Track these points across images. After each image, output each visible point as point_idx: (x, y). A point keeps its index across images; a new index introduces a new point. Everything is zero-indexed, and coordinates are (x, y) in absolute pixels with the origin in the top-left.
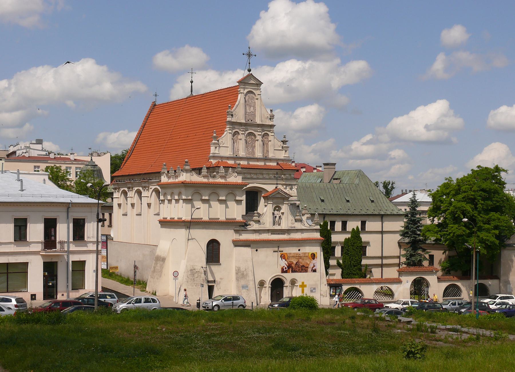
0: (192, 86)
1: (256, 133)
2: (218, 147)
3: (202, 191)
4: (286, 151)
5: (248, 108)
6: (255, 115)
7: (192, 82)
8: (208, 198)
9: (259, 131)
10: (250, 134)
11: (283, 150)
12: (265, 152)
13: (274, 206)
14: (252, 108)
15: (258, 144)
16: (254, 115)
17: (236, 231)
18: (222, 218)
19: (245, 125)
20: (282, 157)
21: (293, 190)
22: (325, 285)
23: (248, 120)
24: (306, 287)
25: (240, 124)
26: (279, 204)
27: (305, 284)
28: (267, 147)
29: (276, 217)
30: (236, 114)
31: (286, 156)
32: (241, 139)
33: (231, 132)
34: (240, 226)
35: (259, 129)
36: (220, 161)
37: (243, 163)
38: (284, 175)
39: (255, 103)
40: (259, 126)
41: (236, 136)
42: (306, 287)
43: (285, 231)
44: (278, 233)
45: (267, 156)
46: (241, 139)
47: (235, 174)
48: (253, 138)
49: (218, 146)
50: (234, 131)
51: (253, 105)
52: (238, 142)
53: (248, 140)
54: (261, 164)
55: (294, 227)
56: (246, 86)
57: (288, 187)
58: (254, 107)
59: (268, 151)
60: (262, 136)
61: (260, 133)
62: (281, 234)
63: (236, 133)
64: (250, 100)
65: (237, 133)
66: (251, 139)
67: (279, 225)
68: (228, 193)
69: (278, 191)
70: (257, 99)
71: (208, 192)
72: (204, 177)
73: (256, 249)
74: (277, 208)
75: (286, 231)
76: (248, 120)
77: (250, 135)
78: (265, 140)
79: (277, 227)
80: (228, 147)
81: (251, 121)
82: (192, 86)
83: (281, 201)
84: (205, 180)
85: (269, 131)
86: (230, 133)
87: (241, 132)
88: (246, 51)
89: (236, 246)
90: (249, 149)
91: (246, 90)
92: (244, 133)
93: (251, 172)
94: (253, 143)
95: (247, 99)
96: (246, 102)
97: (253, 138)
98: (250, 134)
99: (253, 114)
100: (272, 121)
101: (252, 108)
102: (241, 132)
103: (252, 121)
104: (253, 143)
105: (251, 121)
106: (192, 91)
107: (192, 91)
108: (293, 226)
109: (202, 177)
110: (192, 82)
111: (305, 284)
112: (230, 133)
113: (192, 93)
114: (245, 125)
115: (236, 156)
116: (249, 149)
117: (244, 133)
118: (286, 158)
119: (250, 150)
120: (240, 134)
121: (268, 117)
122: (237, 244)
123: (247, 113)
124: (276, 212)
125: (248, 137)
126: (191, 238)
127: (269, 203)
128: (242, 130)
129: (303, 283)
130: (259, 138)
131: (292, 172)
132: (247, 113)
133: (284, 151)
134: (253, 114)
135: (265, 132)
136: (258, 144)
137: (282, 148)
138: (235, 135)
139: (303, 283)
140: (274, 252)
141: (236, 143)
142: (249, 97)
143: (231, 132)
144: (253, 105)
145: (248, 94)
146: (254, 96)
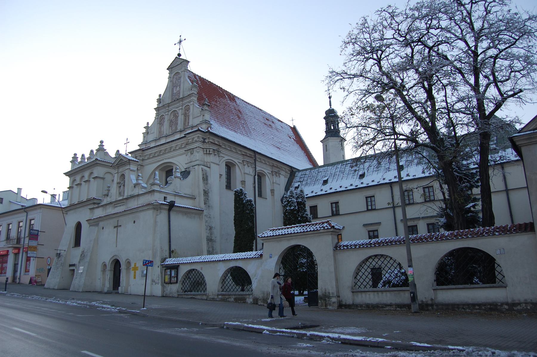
0: (330, 101)
2: (146, 136)
5: (174, 90)
7: (330, 98)
12: (187, 124)
15: (181, 118)
22: (158, 267)
24: (138, 270)
27: (137, 266)
34: (94, 203)
42: (138, 270)
44: (120, 204)
62: (122, 205)
65: (164, 117)
82: (330, 101)
88: (183, 38)
108: (132, 193)
111: (137, 266)
129: (135, 265)
139: (135, 265)
140: (115, 227)
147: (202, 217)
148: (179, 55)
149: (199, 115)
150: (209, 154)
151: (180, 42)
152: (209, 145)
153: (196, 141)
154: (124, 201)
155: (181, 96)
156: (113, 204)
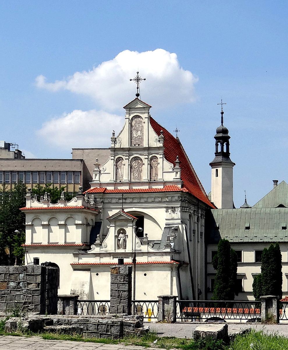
0: (222, 118)
1: (142, 157)
2: (98, 175)
3: (42, 217)
4: (177, 173)
5: (134, 132)
6: (142, 139)
7: (222, 113)
8: (47, 224)
9: (145, 154)
10: (136, 158)
11: (173, 172)
12: (154, 175)
13: (118, 229)
14: (139, 132)
16: (141, 138)
17: (75, 255)
18: (62, 242)
19: (129, 150)
20: (172, 180)
21: (176, 212)
23: (135, 145)
25: (123, 149)
26: (124, 226)
28: (156, 170)
29: (119, 240)
30: (119, 139)
31: (177, 177)
32: (124, 165)
33: (113, 158)
34: (80, 249)
35: (146, 152)
36: (99, 187)
37: (126, 188)
38: (167, 197)
39: (143, 127)
40: (145, 149)
41: (120, 162)
43: (128, 254)
45: (156, 180)
46: (124, 165)
47: (75, 199)
48: (140, 162)
49: (98, 173)
50: (116, 157)
51: (140, 129)
52: (122, 168)
53: (134, 164)
54: (146, 187)
55: (140, 250)
56: (131, 111)
57: (170, 210)
58: (142, 131)
59: (157, 174)
60: (149, 159)
61: (147, 157)
63: (119, 159)
64: (137, 124)
66: (136, 164)
67: (125, 248)
68: (67, 218)
69: (120, 213)
70: (144, 123)
71: (48, 217)
72: (44, 203)
73: (96, 273)
74: (121, 231)
75: (129, 254)
76: (135, 145)
77: (136, 160)
78: (154, 163)
79: (118, 251)
80: (110, 173)
81: (139, 145)
82: (222, 118)
83: (125, 223)
84: (45, 206)
85: (157, 154)
86: (112, 159)
87: (124, 158)
89: (75, 270)
90: (135, 174)
91: (132, 116)
92: (127, 158)
93: (130, 196)
94: (139, 167)
95: (133, 124)
96: (132, 126)
97: (140, 162)
98: (136, 158)
99: (140, 138)
100: (160, 143)
101: (139, 132)
102: (124, 158)
103: (140, 146)
104: (139, 167)
105: (139, 145)
106: (222, 122)
107: (222, 122)
108: (138, 249)
109: (42, 203)
110: (222, 113)
112: (112, 159)
113: (222, 124)
114: (129, 150)
115: (120, 181)
116: (135, 174)
117: (127, 158)
118: (176, 180)
119: (136, 175)
120: (124, 159)
121: (156, 139)
122: (76, 268)
123: (134, 138)
124: (121, 235)
125: (134, 162)
126: (31, 262)
127: (111, 226)
128: (125, 155)
130: (146, 162)
131: (175, 194)
132: (134, 138)
133: (175, 173)
134: (140, 138)
135: (153, 155)
136: (145, 168)
137: (173, 170)
138: (120, 161)
141: (120, 169)
142: (136, 122)
143: (113, 158)
144: (140, 129)
145: (136, 119)
146: (141, 120)
147: (187, 270)
148: (138, 95)
149: (171, 170)
150: (186, 212)
151: (138, 80)
152: (186, 204)
153: (176, 201)
154: (128, 254)
155: (145, 145)
156: (112, 255)
